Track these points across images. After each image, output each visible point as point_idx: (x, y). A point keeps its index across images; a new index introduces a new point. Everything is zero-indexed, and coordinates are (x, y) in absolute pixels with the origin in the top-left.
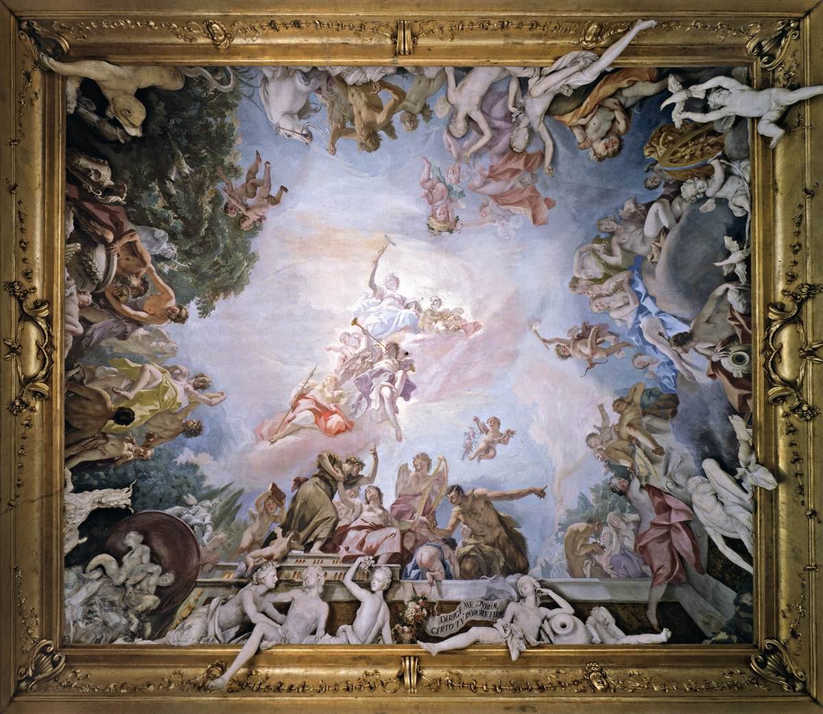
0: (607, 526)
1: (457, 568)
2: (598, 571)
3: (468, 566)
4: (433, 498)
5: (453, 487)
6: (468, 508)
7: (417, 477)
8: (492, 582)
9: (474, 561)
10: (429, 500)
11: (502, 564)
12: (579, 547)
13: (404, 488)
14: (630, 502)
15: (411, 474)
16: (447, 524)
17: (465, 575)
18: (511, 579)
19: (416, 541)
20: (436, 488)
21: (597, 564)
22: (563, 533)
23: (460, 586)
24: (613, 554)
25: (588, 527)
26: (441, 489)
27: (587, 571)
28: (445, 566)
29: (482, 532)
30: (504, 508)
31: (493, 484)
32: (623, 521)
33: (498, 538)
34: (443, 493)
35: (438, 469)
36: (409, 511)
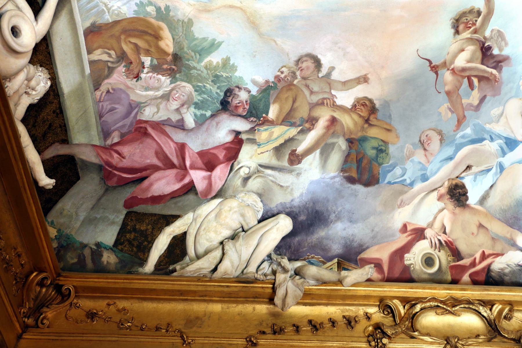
0: (171, 83)
2: (99, 74)
12: (133, 40)
14: (213, 116)
21: (111, 70)
22: (154, 13)
24: (129, 92)
25: (166, 54)
27: (99, 55)
32: (183, 105)
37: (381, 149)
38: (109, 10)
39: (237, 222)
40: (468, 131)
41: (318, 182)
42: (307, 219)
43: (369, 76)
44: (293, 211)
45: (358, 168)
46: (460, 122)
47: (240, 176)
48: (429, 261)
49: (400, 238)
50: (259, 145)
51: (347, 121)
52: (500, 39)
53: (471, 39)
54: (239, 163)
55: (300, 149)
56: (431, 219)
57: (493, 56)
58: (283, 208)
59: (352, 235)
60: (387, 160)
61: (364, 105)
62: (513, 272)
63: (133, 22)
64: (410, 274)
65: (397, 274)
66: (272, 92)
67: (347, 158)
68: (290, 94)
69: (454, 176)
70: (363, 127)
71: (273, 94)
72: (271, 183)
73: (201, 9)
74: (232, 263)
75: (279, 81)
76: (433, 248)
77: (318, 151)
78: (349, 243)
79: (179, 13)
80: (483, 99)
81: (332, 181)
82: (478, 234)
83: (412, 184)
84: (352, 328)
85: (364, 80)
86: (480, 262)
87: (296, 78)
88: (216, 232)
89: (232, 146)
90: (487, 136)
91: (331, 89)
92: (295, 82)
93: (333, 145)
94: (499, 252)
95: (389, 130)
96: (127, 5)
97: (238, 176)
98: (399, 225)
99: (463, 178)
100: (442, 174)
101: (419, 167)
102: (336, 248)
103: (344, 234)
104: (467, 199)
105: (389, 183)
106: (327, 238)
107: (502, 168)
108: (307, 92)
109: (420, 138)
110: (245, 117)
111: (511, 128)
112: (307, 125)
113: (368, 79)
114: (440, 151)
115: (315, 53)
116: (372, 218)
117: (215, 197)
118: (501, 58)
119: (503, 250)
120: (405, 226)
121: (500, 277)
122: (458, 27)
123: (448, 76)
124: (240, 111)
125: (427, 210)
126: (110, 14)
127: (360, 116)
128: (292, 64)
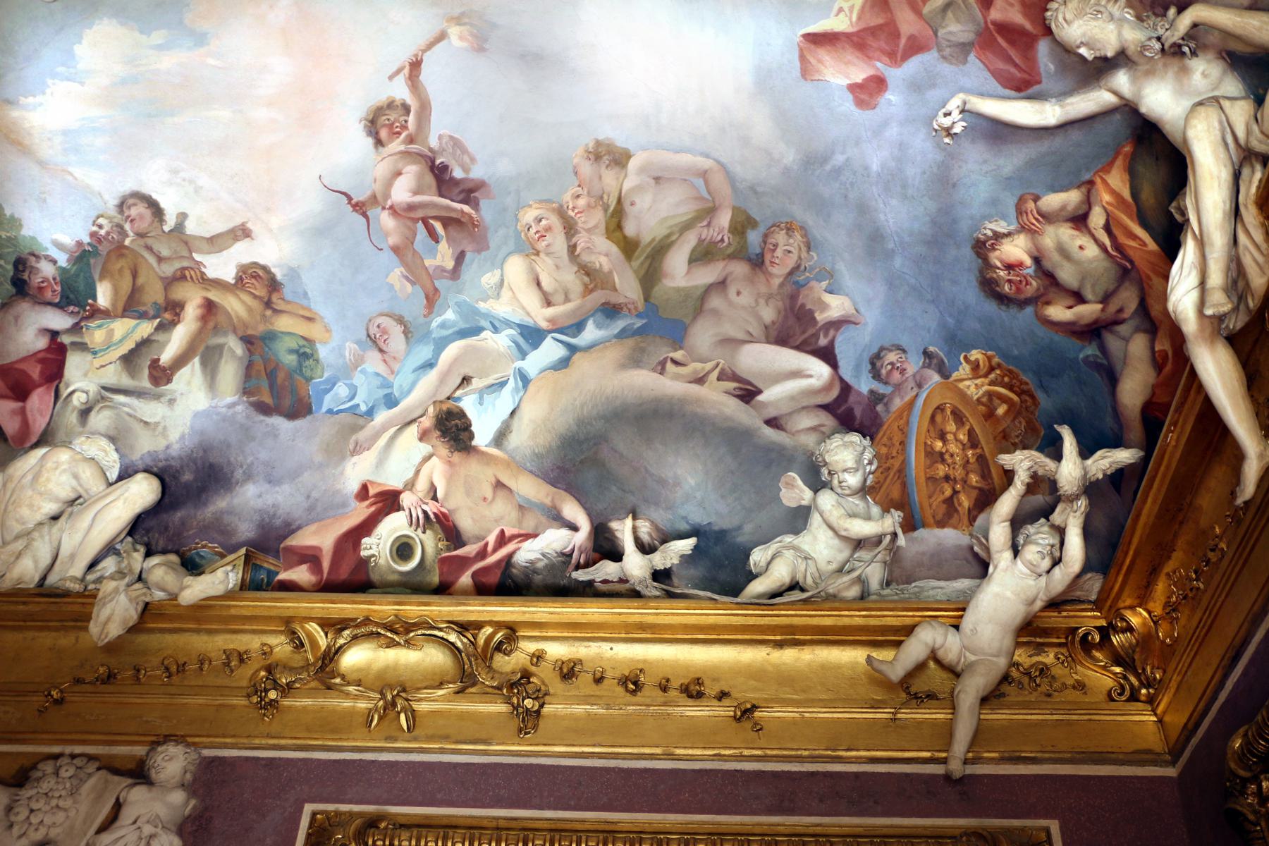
37: (305, 353)
39: (68, 488)
40: (450, 315)
41: (205, 414)
42: (195, 480)
43: (249, 225)
44: (170, 466)
45: (271, 386)
46: (432, 300)
47: (75, 408)
48: (403, 549)
49: (355, 509)
50: (95, 353)
51: (235, 305)
52: (459, 152)
53: (406, 154)
54: (67, 386)
55: (167, 356)
56: (410, 474)
57: (455, 182)
58: (154, 460)
59: (274, 505)
60: (319, 372)
61: (256, 276)
62: (551, 567)
64: (367, 573)
65: (344, 574)
66: (92, 261)
67: (249, 371)
68: (122, 263)
69: (442, 397)
70: (264, 316)
71: (96, 266)
72: (127, 418)
74: (36, 562)
75: (99, 241)
76: (414, 527)
77: (197, 360)
78: (267, 520)
80: (460, 258)
81: (231, 411)
82: (494, 498)
83: (370, 413)
84: (232, 671)
85: (242, 233)
86: (495, 550)
87: (127, 236)
88: (31, 506)
89: (49, 356)
90: (484, 323)
91: (191, 252)
92: (127, 242)
93: (220, 348)
94: (530, 531)
95: (310, 319)
97: (70, 408)
98: (354, 487)
99: (459, 399)
100: (421, 393)
101: (378, 381)
102: (246, 530)
103: (259, 504)
104: (472, 436)
105: (330, 411)
106: (230, 512)
107: (525, 380)
108: (152, 260)
109: (367, 330)
110: (59, 306)
111: (524, 308)
112: (167, 316)
113: (250, 231)
114: (408, 353)
115: (147, 189)
116: (306, 474)
117: (37, 445)
118: (470, 185)
119: (537, 527)
120: (365, 487)
121: (527, 576)
122: (377, 133)
123: (386, 220)
124: (48, 295)
125: (404, 460)
127: (255, 297)
128: (112, 212)
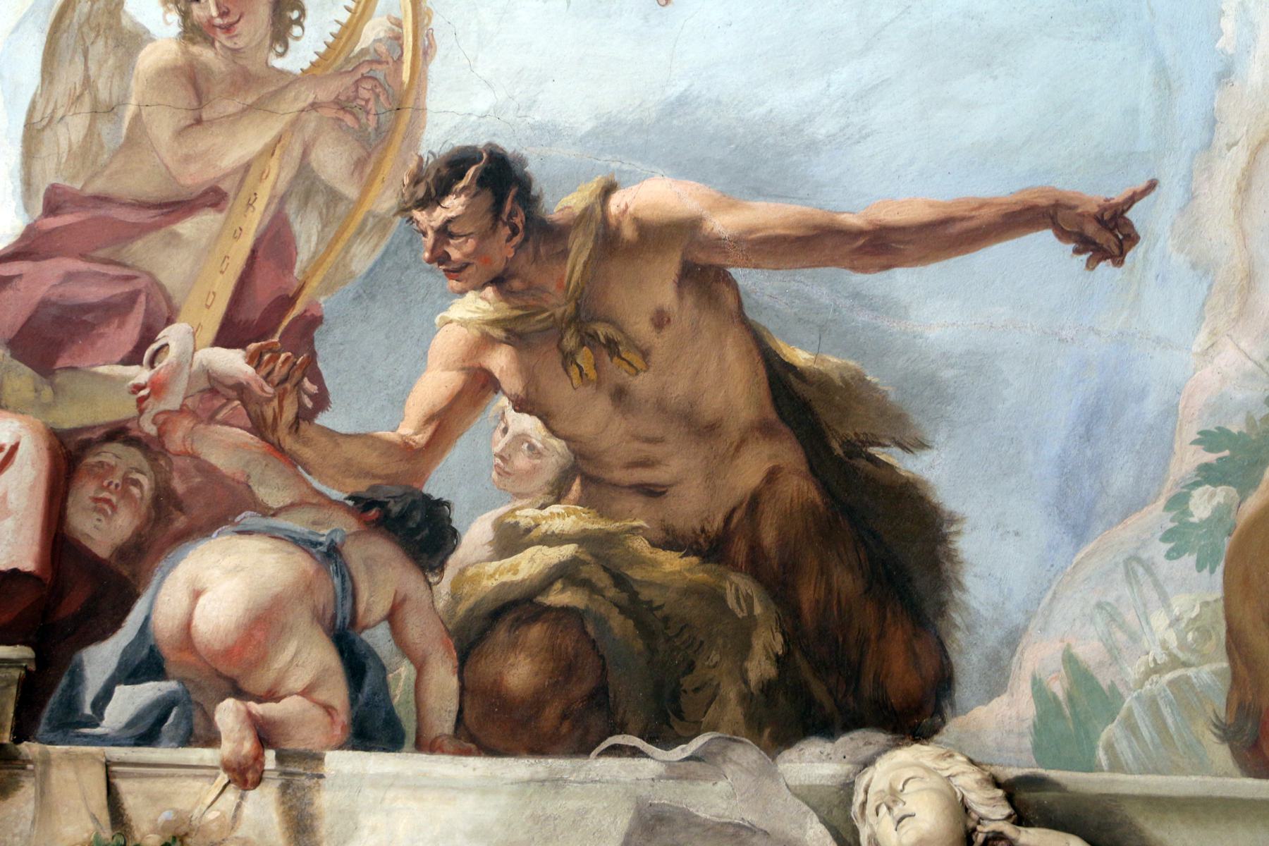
1: (444, 682)
3: (519, 672)
4: (307, 234)
5: (457, 163)
6: (560, 307)
7: (192, 79)
8: (675, 773)
9: (569, 642)
10: (274, 244)
11: (760, 668)
13: (87, 150)
15: (149, 59)
16: (398, 403)
17: (490, 726)
18: (814, 764)
19: (164, 503)
20: (332, 161)
22: (1222, 494)
23: (447, 787)
26: (365, 165)
28: (356, 662)
29: (646, 463)
30: (810, 318)
31: (749, 159)
33: (754, 503)
34: (385, 200)
35: (350, 30)
36: (115, 310)
38: (1175, 663)
63: (1246, 580)
73: (1234, 309)
79: (1239, 396)
96: (1169, 589)
126: (1193, 659)
